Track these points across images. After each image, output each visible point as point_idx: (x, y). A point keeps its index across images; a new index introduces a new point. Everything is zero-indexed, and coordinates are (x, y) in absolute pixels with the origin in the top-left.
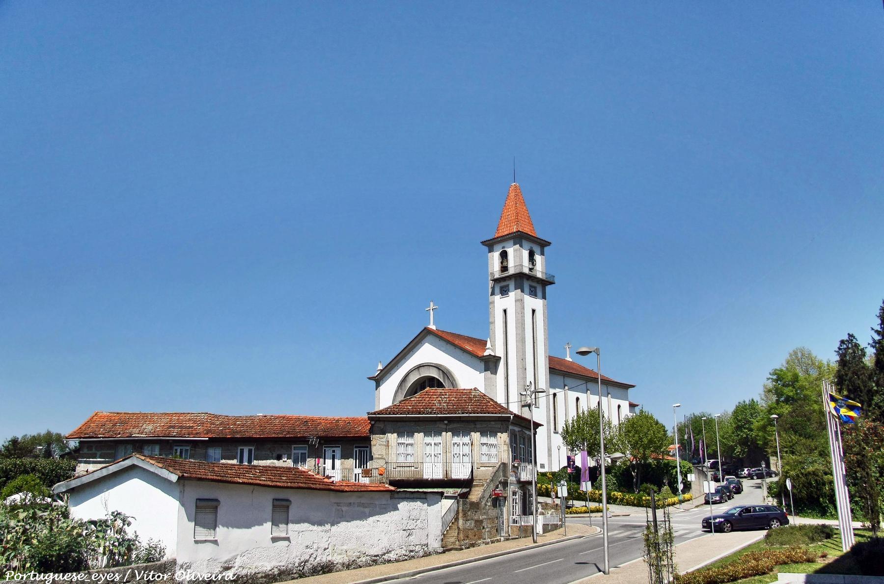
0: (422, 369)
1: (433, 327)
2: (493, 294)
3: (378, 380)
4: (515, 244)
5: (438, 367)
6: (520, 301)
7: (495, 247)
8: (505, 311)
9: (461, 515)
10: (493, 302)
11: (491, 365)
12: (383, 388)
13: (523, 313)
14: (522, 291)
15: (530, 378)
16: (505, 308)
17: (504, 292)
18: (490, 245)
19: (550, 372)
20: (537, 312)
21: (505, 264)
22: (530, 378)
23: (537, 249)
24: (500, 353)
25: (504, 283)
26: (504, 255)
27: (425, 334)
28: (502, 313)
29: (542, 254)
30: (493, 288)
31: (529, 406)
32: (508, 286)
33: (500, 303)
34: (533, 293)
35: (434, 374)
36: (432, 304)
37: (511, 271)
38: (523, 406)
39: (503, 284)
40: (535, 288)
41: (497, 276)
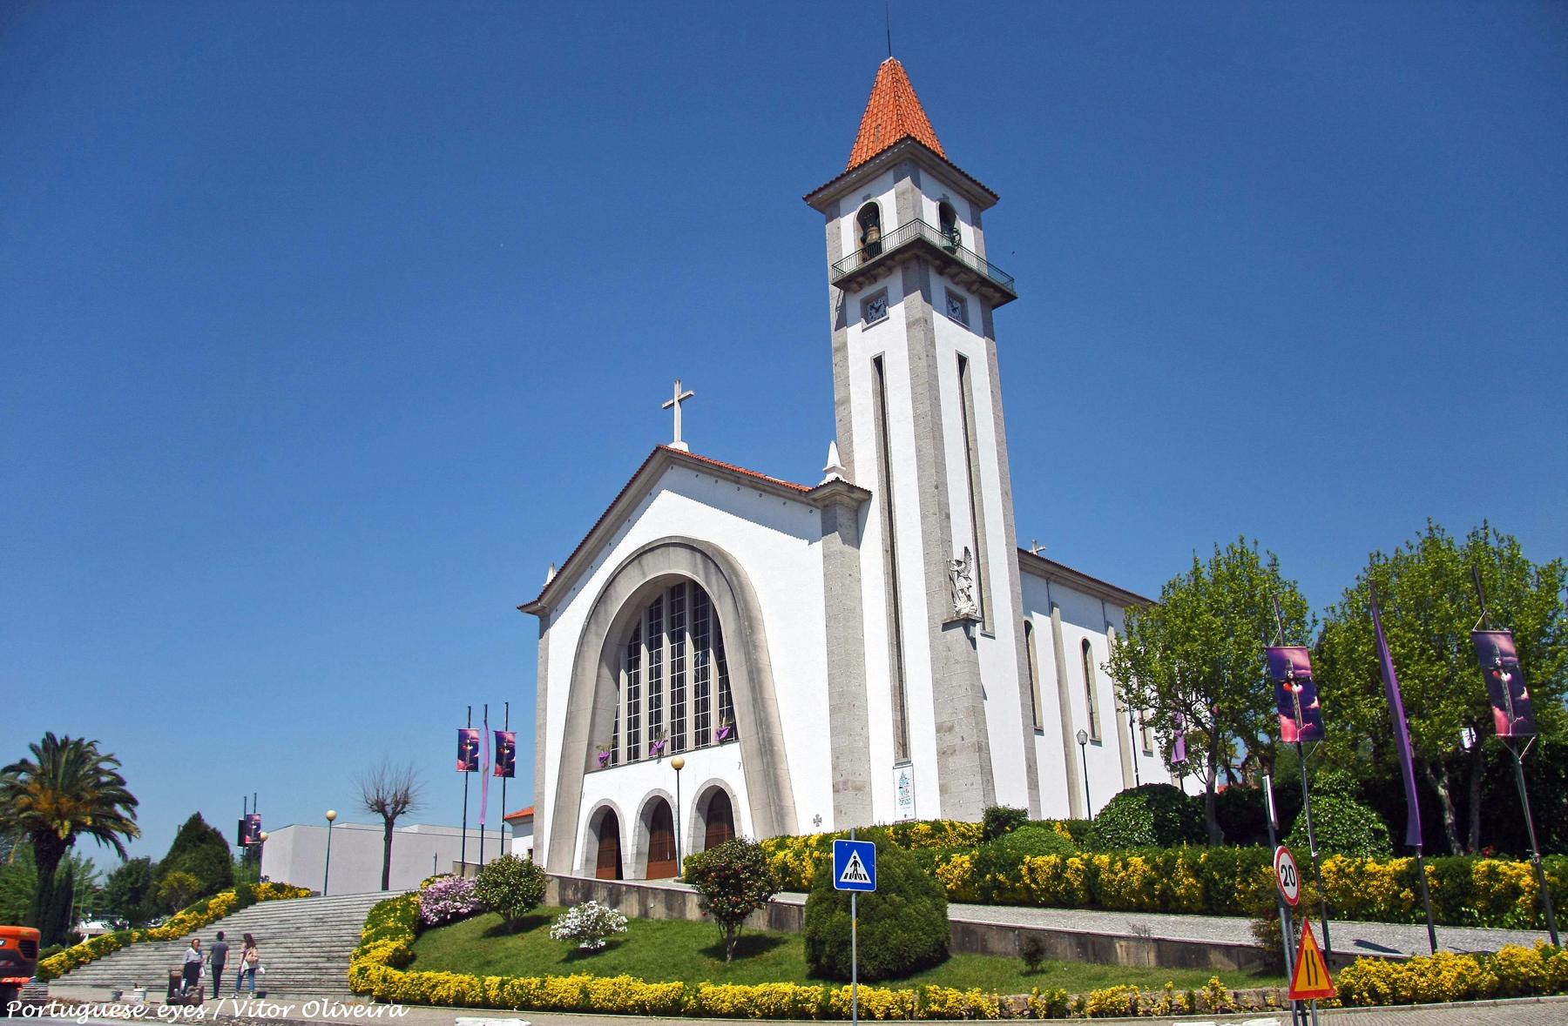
0: (649, 558)
1: (679, 445)
2: (842, 323)
3: (544, 611)
4: (898, 179)
5: (689, 546)
6: (919, 327)
7: (843, 204)
8: (878, 362)
9: (237, 852)
10: (843, 347)
11: (843, 516)
12: (554, 631)
13: (932, 366)
14: (927, 298)
15: (961, 537)
16: (876, 353)
17: (874, 311)
18: (826, 204)
19: (1023, 567)
20: (972, 364)
21: (873, 237)
22: (961, 537)
23: (959, 205)
24: (866, 476)
25: (868, 287)
26: (870, 217)
27: (658, 467)
28: (869, 369)
29: (976, 222)
30: (842, 309)
31: (967, 622)
32: (883, 293)
33: (859, 343)
34: (957, 312)
35: (681, 566)
36: (677, 388)
37: (890, 245)
38: (947, 626)
39: (869, 291)
40: (962, 301)
41: (851, 266)
